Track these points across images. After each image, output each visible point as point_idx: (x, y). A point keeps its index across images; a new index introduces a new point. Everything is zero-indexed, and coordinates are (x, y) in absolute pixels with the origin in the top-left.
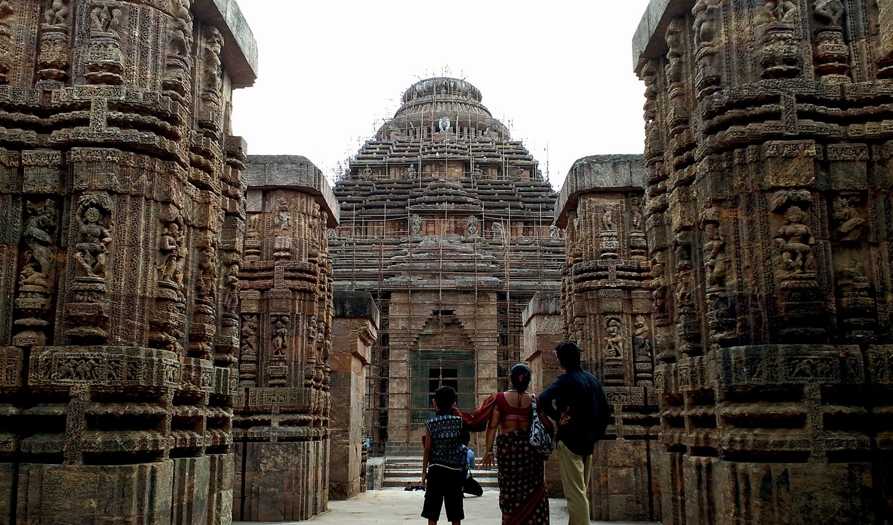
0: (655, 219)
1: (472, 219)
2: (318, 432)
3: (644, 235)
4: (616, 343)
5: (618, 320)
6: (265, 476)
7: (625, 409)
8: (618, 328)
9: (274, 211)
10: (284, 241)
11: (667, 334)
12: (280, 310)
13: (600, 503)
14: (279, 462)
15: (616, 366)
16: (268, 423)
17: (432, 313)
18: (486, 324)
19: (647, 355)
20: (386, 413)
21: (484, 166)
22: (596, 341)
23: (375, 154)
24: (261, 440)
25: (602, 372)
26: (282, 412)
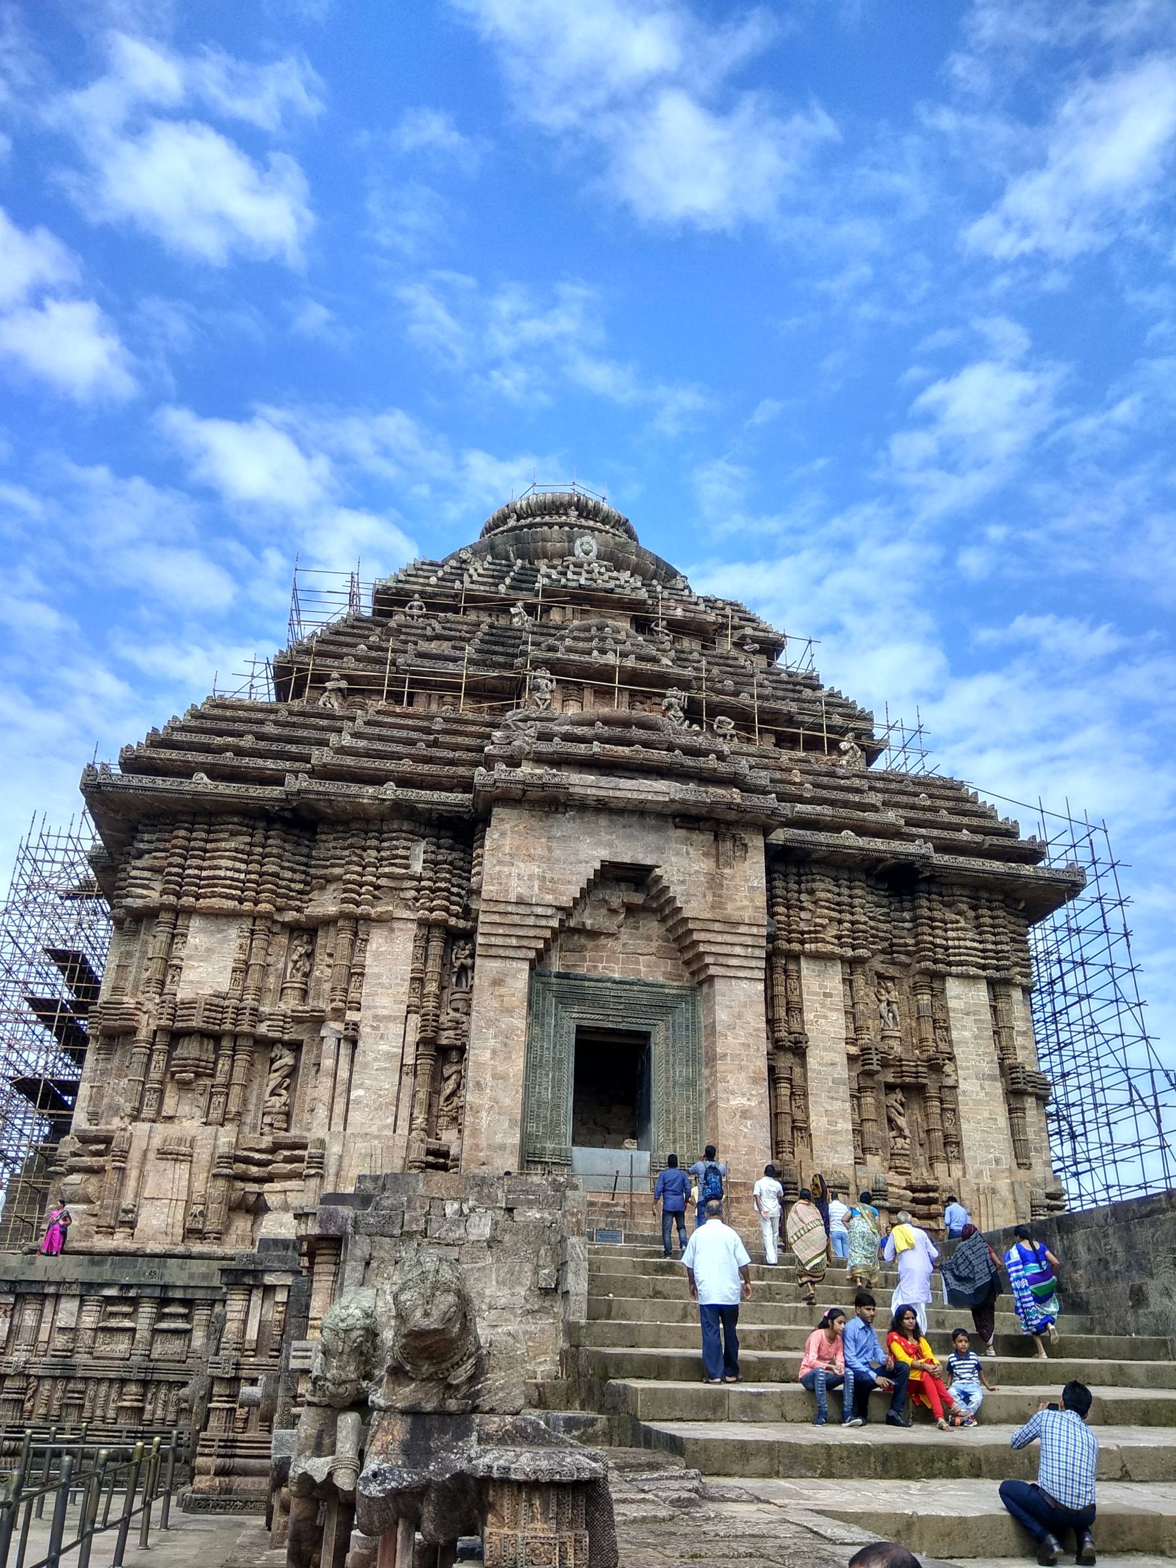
1: (675, 696)
17: (598, 866)
18: (738, 909)
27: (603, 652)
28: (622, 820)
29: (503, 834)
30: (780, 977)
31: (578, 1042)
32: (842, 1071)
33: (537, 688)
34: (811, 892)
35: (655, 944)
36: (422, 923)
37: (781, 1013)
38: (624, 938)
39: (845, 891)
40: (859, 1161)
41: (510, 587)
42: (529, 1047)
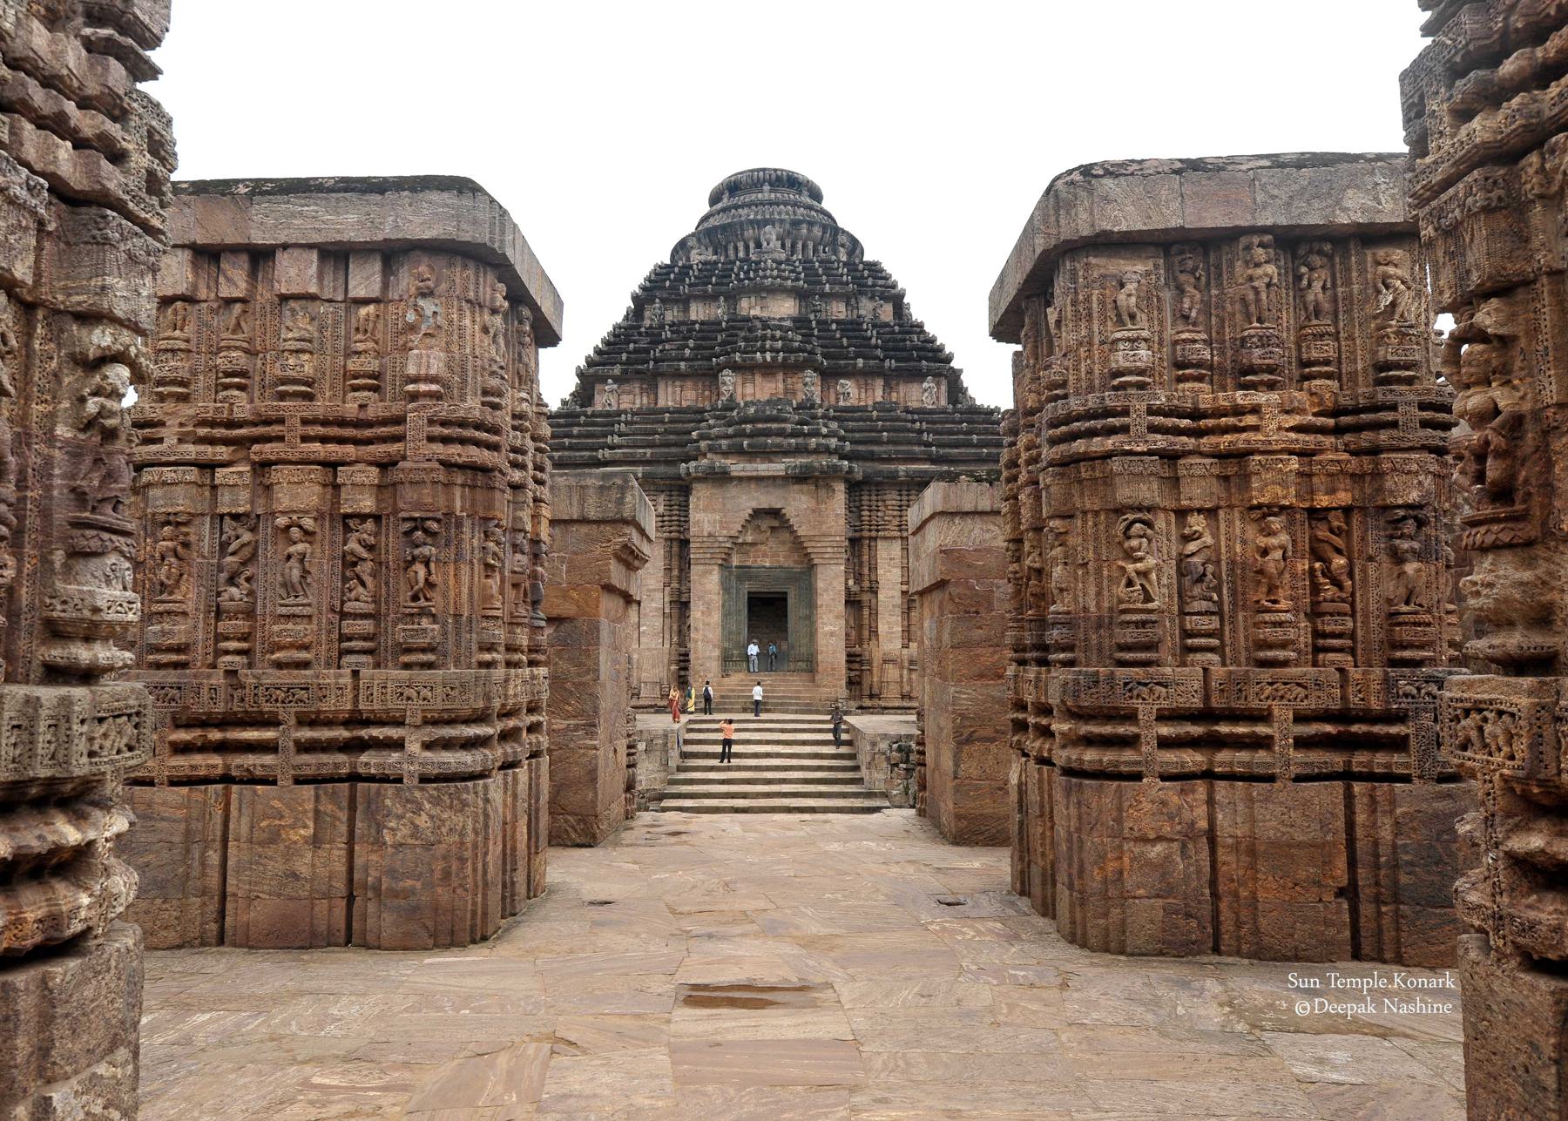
0: (1489, 184)
2: (515, 752)
3: (1204, 336)
4: (1144, 574)
5: (1149, 524)
6: (393, 855)
7: (1164, 717)
8: (1150, 541)
9: (405, 297)
10: (427, 359)
11: (1527, 575)
12: (418, 505)
13: (1106, 915)
14: (423, 825)
15: (1144, 624)
16: (399, 745)
17: (750, 512)
19: (1210, 599)
20: (687, 655)
21: (823, 296)
22: (1099, 571)
23: (668, 283)
24: (385, 779)
25: (1111, 636)
26: (427, 722)
27: (763, 351)
28: (763, 484)
29: (698, 499)
30: (866, 550)
31: (750, 599)
32: (898, 600)
33: (724, 384)
34: (884, 501)
35: (788, 546)
36: (666, 539)
37: (866, 571)
38: (770, 544)
39: (904, 498)
40: (905, 646)
41: (717, 284)
42: (723, 606)
